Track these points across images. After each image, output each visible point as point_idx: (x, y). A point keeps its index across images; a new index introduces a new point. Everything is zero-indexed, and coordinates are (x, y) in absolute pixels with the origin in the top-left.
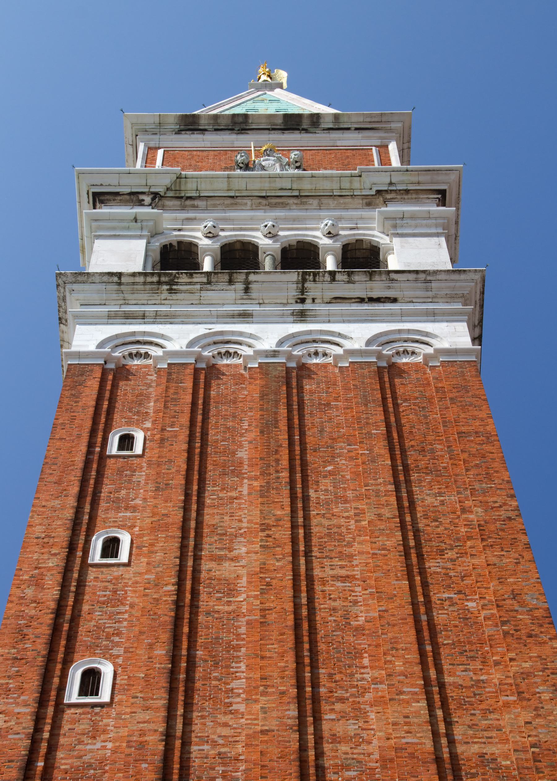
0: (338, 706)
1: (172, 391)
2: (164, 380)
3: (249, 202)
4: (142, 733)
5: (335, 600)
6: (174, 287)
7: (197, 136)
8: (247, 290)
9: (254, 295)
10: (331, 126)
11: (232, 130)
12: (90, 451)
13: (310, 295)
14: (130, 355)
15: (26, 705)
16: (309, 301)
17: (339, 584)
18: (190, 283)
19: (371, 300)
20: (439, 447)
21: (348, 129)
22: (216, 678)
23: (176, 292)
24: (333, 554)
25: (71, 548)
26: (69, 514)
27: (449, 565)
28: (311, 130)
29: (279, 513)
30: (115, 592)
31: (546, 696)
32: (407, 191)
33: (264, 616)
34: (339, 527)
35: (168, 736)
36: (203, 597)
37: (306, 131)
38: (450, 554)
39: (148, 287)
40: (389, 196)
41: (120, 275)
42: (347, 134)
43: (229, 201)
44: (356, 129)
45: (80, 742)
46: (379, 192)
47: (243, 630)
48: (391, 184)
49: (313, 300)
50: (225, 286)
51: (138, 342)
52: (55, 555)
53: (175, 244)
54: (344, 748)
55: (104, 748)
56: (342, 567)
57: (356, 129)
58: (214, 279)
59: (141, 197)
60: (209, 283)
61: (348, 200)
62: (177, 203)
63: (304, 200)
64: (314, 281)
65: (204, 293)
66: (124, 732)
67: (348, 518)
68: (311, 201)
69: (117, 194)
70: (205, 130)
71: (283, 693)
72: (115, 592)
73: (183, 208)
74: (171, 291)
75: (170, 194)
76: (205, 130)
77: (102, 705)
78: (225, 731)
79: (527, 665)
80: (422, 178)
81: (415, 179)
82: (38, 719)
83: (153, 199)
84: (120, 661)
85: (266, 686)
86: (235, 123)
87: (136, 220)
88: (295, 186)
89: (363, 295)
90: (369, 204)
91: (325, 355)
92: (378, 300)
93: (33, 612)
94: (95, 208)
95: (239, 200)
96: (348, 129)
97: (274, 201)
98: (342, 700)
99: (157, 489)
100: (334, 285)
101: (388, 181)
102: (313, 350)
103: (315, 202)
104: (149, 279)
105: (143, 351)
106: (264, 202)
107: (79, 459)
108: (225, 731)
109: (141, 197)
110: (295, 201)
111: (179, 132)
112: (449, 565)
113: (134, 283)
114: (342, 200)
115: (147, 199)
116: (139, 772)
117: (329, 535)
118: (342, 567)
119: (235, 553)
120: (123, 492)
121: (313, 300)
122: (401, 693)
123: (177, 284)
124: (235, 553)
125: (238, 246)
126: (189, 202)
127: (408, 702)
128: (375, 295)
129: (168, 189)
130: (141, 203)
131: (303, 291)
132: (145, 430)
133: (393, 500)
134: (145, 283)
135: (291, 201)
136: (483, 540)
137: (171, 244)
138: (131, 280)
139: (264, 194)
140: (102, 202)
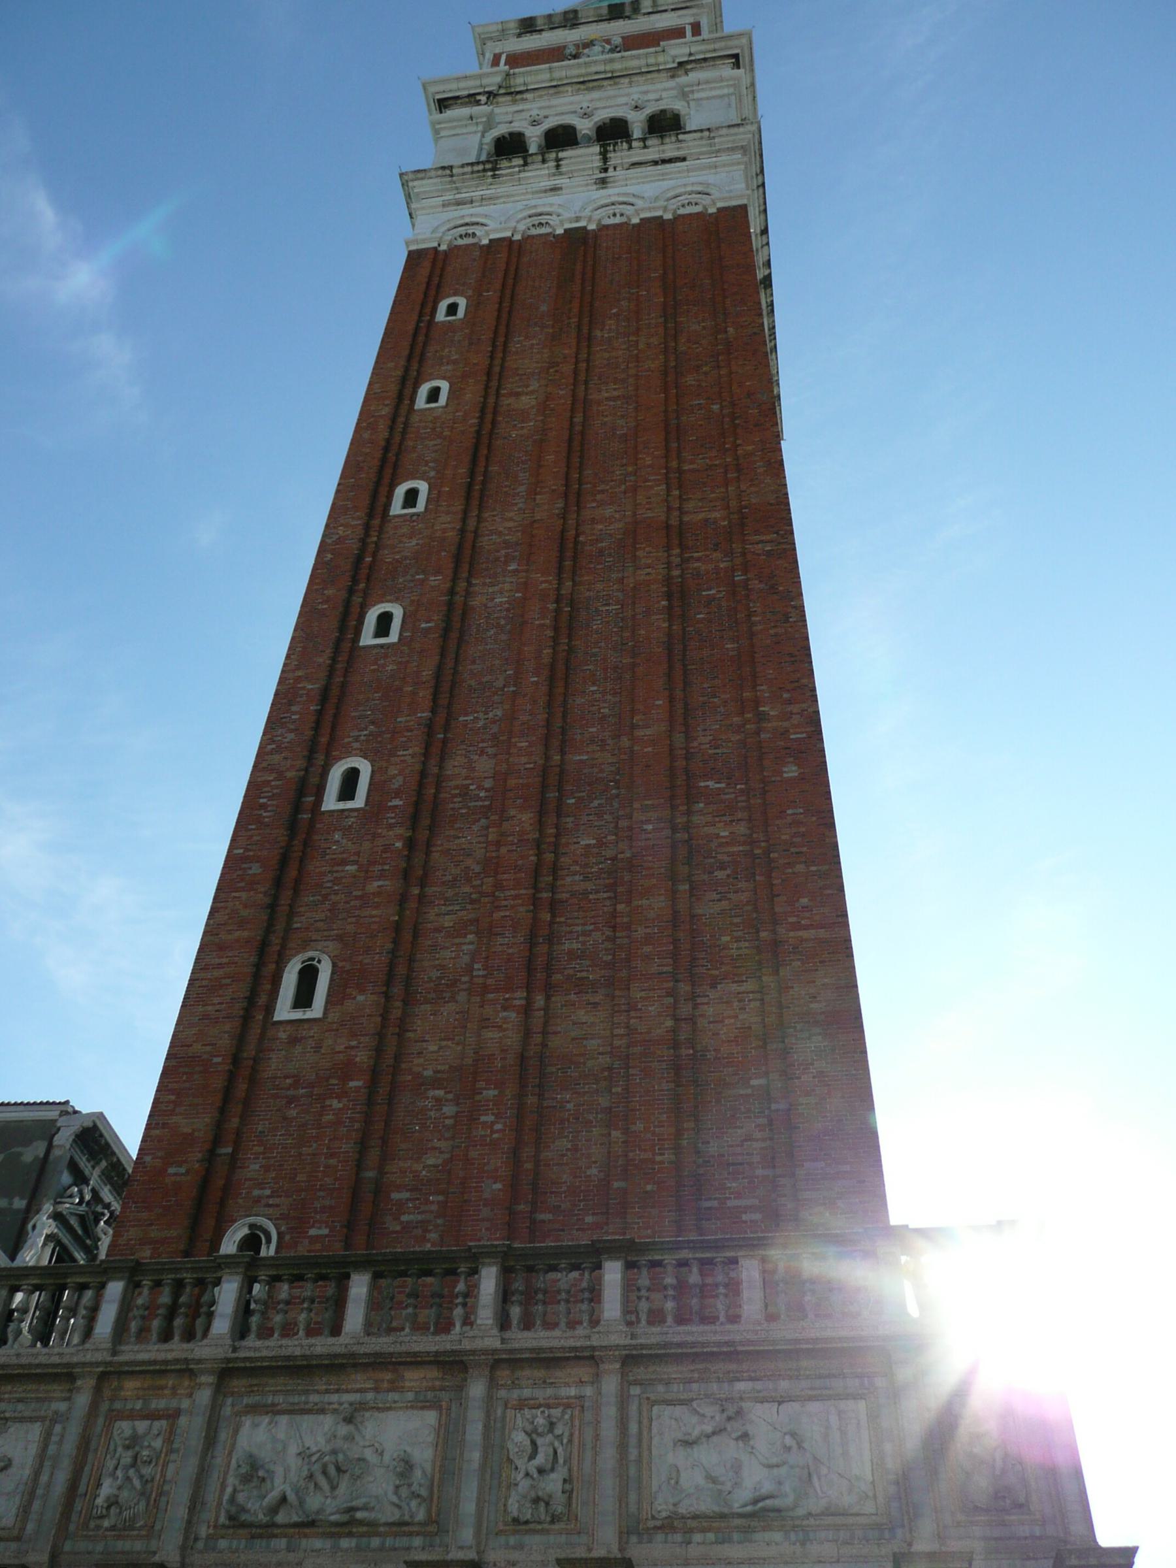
3: (569, 89)
4: (444, 531)
5: (607, 416)
6: (497, 172)
7: (535, 36)
8: (558, 166)
9: (563, 169)
10: (650, 10)
11: (565, 26)
13: (612, 163)
14: (461, 236)
15: (359, 518)
16: (611, 169)
18: (510, 167)
19: (664, 161)
21: (665, 11)
22: (506, 486)
23: (499, 176)
25: (400, 397)
26: (399, 373)
28: (635, 16)
29: (566, 352)
32: (705, 60)
35: (462, 531)
37: (629, 18)
39: (475, 175)
40: (689, 67)
42: (664, 15)
43: (552, 91)
44: (673, 10)
45: (401, 542)
46: (681, 64)
48: (691, 54)
49: (615, 168)
50: (540, 166)
51: (467, 224)
52: (387, 405)
53: (507, 136)
56: (615, 389)
57: (673, 10)
59: (478, 98)
61: (655, 75)
62: (509, 98)
63: (617, 80)
64: (614, 150)
65: (522, 175)
68: (622, 80)
69: (457, 98)
70: (542, 30)
73: (514, 102)
74: (494, 176)
75: (502, 91)
76: (542, 30)
79: (750, 448)
80: (717, 46)
81: (711, 47)
82: (367, 527)
83: (488, 98)
86: (566, 20)
87: (471, 118)
88: (608, 68)
89: (656, 157)
91: (622, 215)
92: (670, 161)
94: (441, 112)
95: (561, 89)
96: (665, 11)
98: (602, 492)
99: (471, 344)
100: (632, 152)
101: (687, 51)
102: (612, 211)
103: (626, 80)
104: (476, 168)
105: (470, 232)
106: (582, 87)
107: (411, 328)
110: (611, 82)
111: (519, 35)
113: (464, 174)
114: (649, 76)
115: (483, 98)
118: (615, 389)
121: (615, 168)
122: (647, 480)
125: (560, 131)
126: (519, 97)
128: (668, 155)
129: (500, 87)
130: (478, 103)
131: (605, 159)
133: (661, 330)
134: (473, 172)
135: (605, 83)
137: (503, 137)
138: (461, 170)
139: (582, 80)
140: (446, 107)
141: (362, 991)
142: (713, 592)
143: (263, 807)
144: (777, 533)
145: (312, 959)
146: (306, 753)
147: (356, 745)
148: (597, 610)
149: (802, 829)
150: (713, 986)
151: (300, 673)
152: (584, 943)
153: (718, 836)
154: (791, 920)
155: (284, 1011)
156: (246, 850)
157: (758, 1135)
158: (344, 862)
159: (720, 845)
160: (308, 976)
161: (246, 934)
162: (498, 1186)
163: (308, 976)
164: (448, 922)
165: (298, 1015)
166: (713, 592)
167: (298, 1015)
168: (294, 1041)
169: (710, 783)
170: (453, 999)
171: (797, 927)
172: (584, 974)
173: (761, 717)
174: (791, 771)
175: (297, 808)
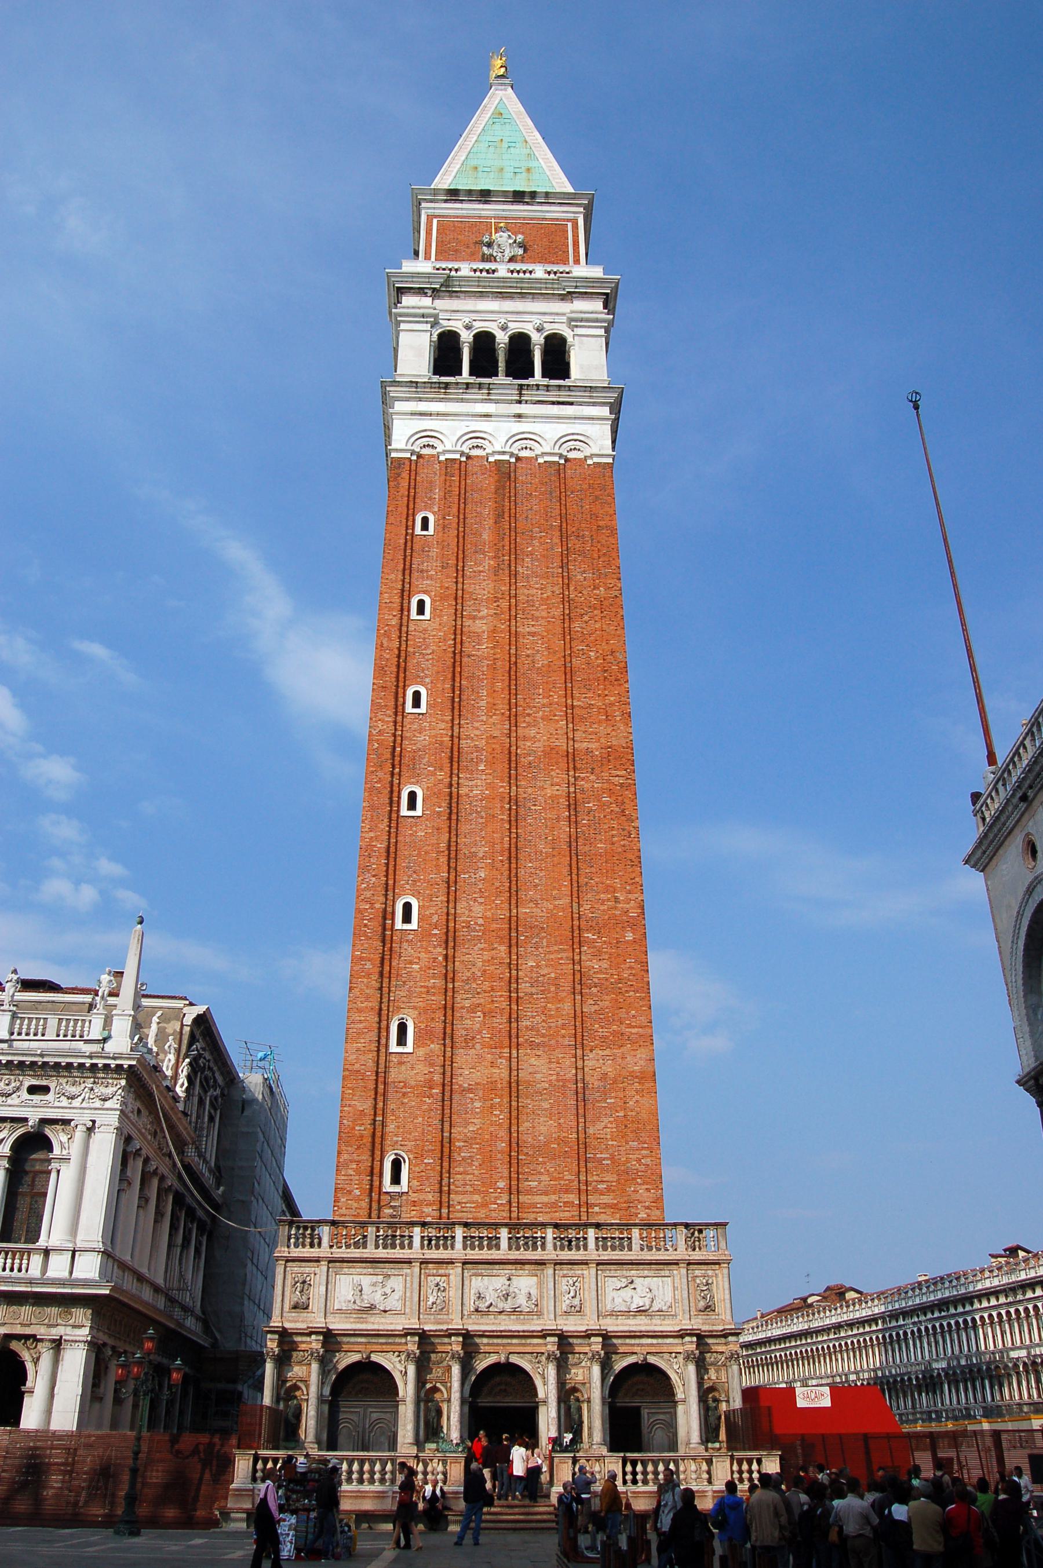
0: (527, 719)
1: (448, 484)
2: (444, 469)
12: (407, 534)
17: (531, 638)
20: (587, 533)
24: (529, 616)
27: (584, 625)
30: (424, 639)
31: (618, 718)
32: (586, 293)
33: (495, 664)
34: (533, 596)
36: (466, 645)
38: (586, 618)
41: (417, 383)
47: (485, 669)
52: (394, 616)
54: (529, 744)
55: (425, 740)
58: (470, 386)
59: (426, 291)
60: (467, 388)
66: (433, 732)
67: (537, 589)
71: (503, 714)
72: (424, 639)
77: (423, 714)
78: (477, 732)
79: (612, 699)
83: (433, 292)
84: (429, 686)
85: (495, 710)
90: (562, 300)
93: (388, 656)
97: (505, 295)
98: (529, 715)
102: (524, 446)
106: (500, 296)
108: (477, 732)
109: (426, 291)
112: (584, 625)
115: (429, 292)
116: (441, 758)
117: (528, 601)
119: (481, 614)
120: (425, 564)
122: (555, 715)
123: (449, 389)
124: (481, 614)
127: (557, 721)
132: (434, 513)
136: (602, 612)
141: (433, 1042)
142: (591, 805)
143: (366, 925)
144: (626, 770)
145: (403, 1019)
146: (384, 893)
147: (408, 887)
148: (530, 809)
149: (633, 972)
150: (591, 1051)
151: (372, 834)
152: (532, 1022)
153: (593, 968)
154: (627, 1022)
155: (394, 1048)
156: (362, 953)
157: (609, 1125)
158: (411, 963)
159: (594, 973)
160: (402, 1028)
161: (370, 1004)
162: (504, 1145)
163: (402, 1028)
164: (467, 1003)
165: (400, 1049)
166: (591, 805)
167: (400, 1049)
168: (401, 1063)
169: (590, 935)
170: (473, 1047)
171: (630, 1026)
172: (533, 1039)
173: (616, 900)
174: (629, 936)
175: (384, 929)
